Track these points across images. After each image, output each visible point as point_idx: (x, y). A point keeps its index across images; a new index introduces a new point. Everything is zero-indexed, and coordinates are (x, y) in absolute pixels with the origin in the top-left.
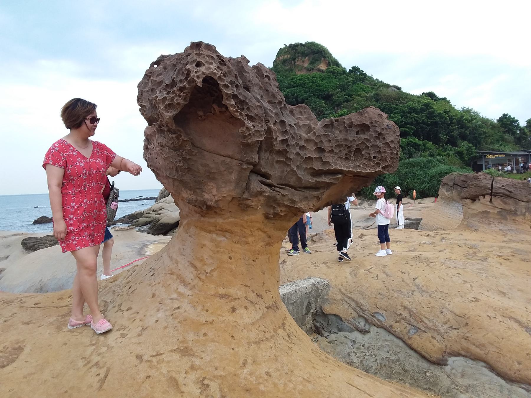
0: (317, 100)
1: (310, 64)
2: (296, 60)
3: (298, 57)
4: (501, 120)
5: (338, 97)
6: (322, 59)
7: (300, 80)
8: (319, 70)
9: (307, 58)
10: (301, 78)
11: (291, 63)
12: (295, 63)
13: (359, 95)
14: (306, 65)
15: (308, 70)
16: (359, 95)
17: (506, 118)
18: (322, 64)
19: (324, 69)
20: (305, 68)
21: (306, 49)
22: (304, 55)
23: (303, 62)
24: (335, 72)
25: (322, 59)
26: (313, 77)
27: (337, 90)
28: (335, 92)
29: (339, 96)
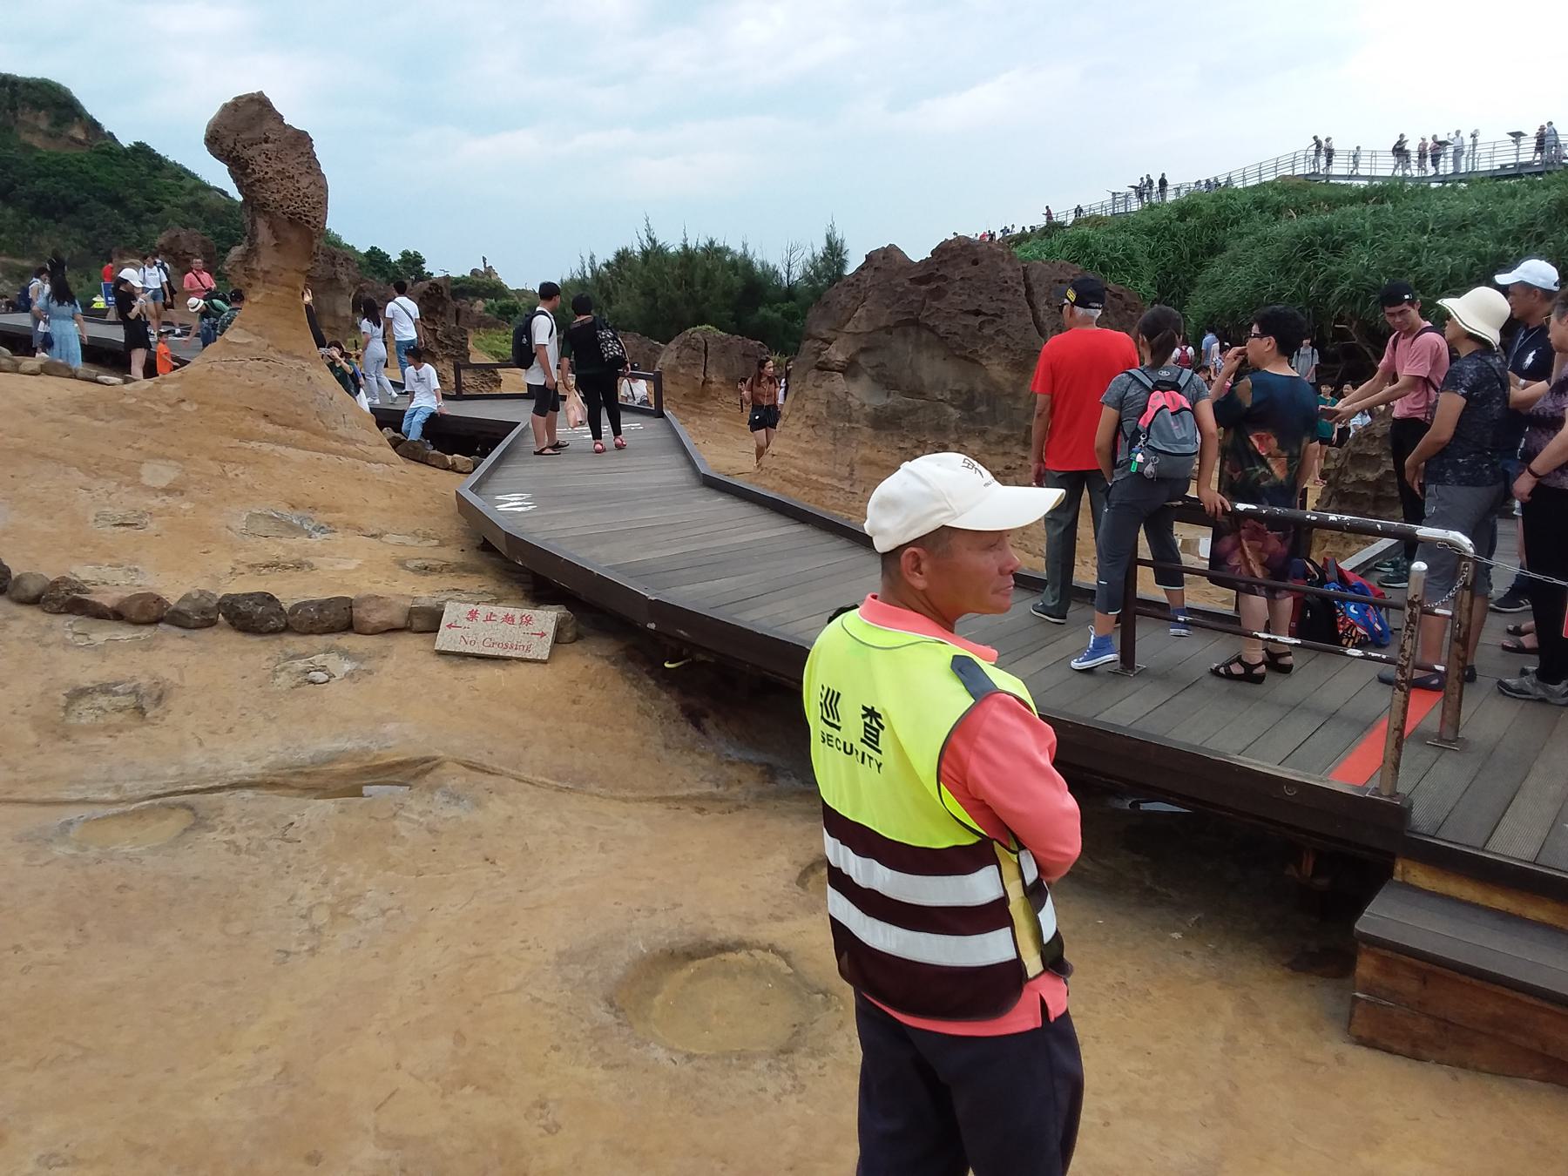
0: (102, 206)
1: (52, 125)
2: (20, 109)
3: (24, 107)
4: (368, 254)
5: (137, 203)
6: (76, 119)
7: (57, 163)
8: (73, 139)
9: (43, 112)
10: (54, 158)
11: (5, 112)
12: (15, 116)
13: (168, 202)
14: (44, 124)
15: (50, 135)
16: (168, 202)
17: (374, 253)
18: (76, 127)
19: (81, 136)
20: (41, 130)
21: (39, 95)
22: (37, 106)
23: (37, 118)
24: (112, 154)
25: (76, 119)
26: (79, 161)
27: (132, 191)
28: (127, 193)
29: (137, 202)
